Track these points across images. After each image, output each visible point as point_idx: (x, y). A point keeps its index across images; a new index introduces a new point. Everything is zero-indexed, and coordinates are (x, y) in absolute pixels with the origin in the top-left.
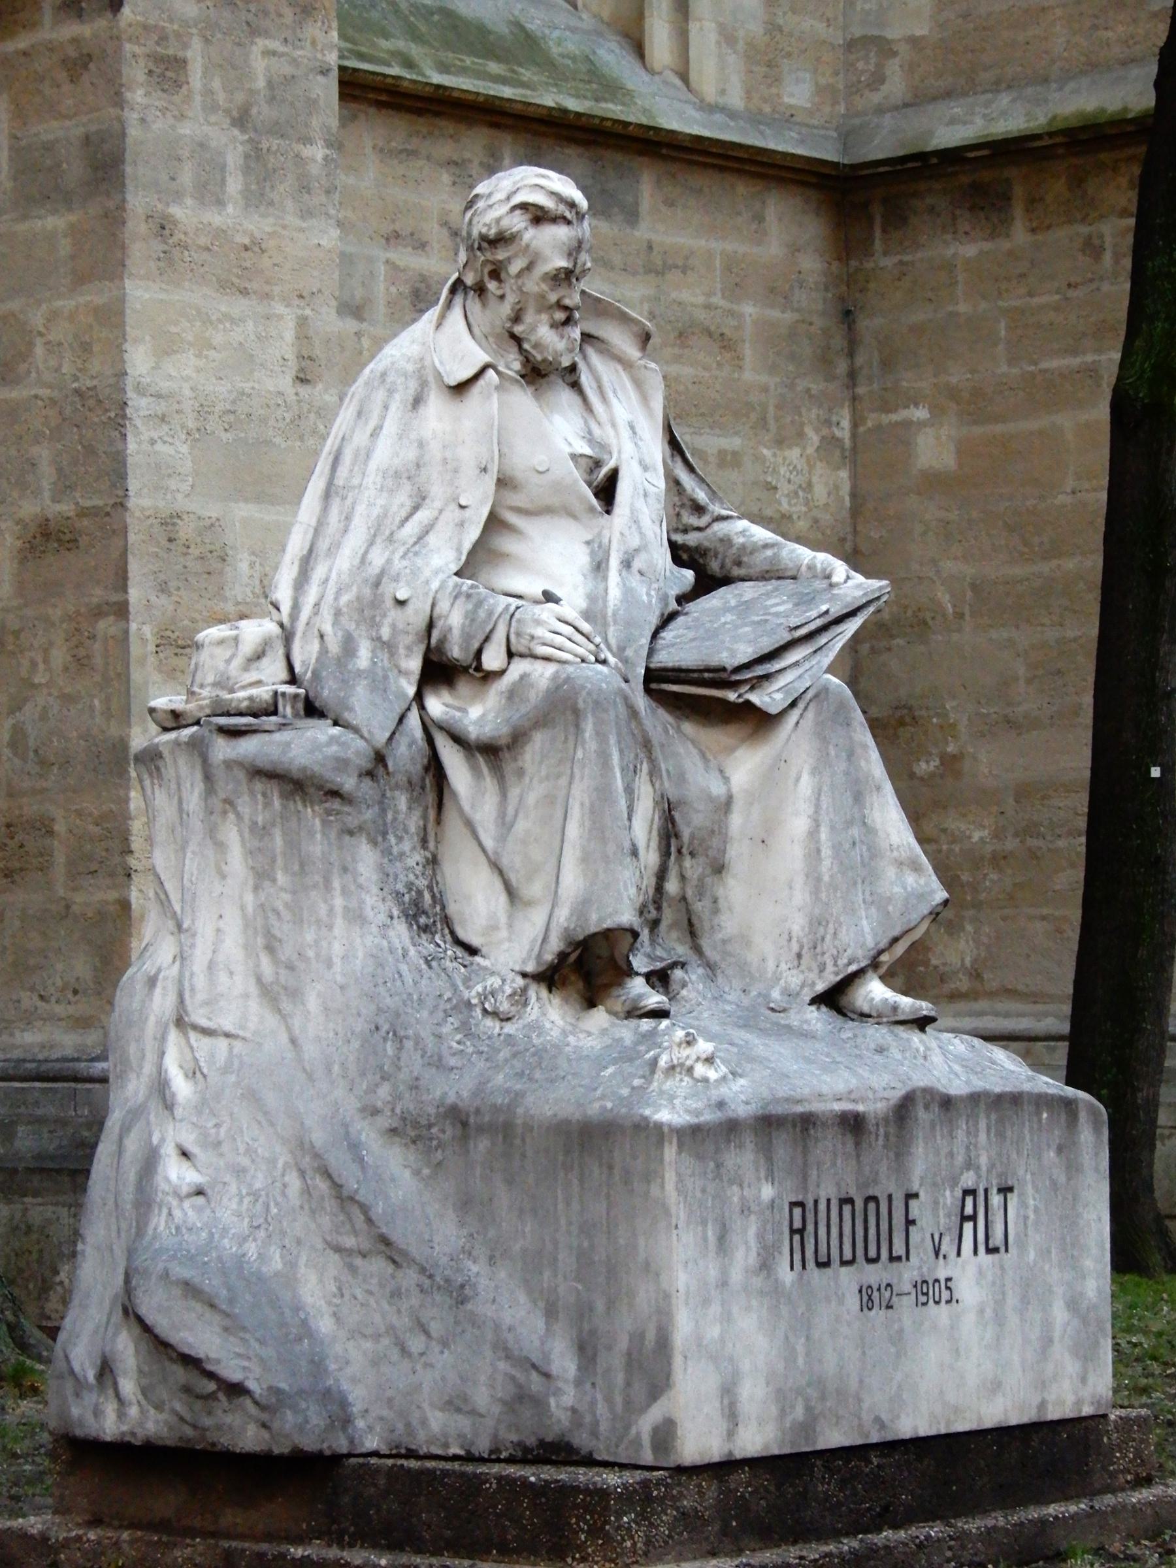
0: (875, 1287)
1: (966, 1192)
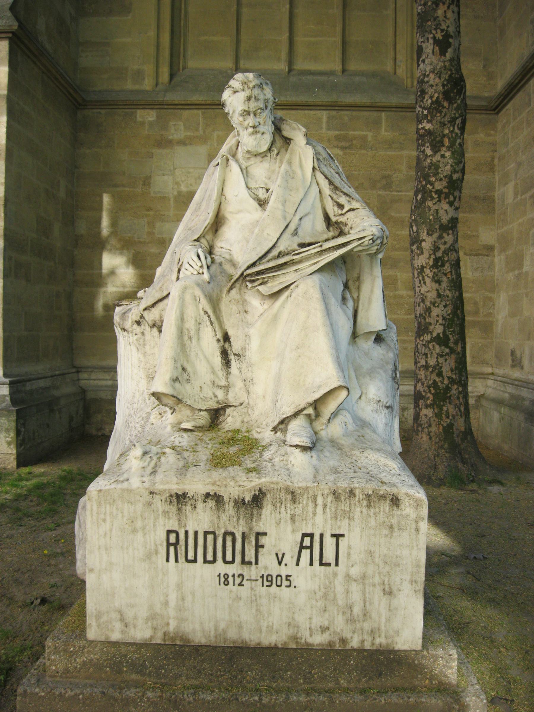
0: (230, 575)
1: (304, 535)
